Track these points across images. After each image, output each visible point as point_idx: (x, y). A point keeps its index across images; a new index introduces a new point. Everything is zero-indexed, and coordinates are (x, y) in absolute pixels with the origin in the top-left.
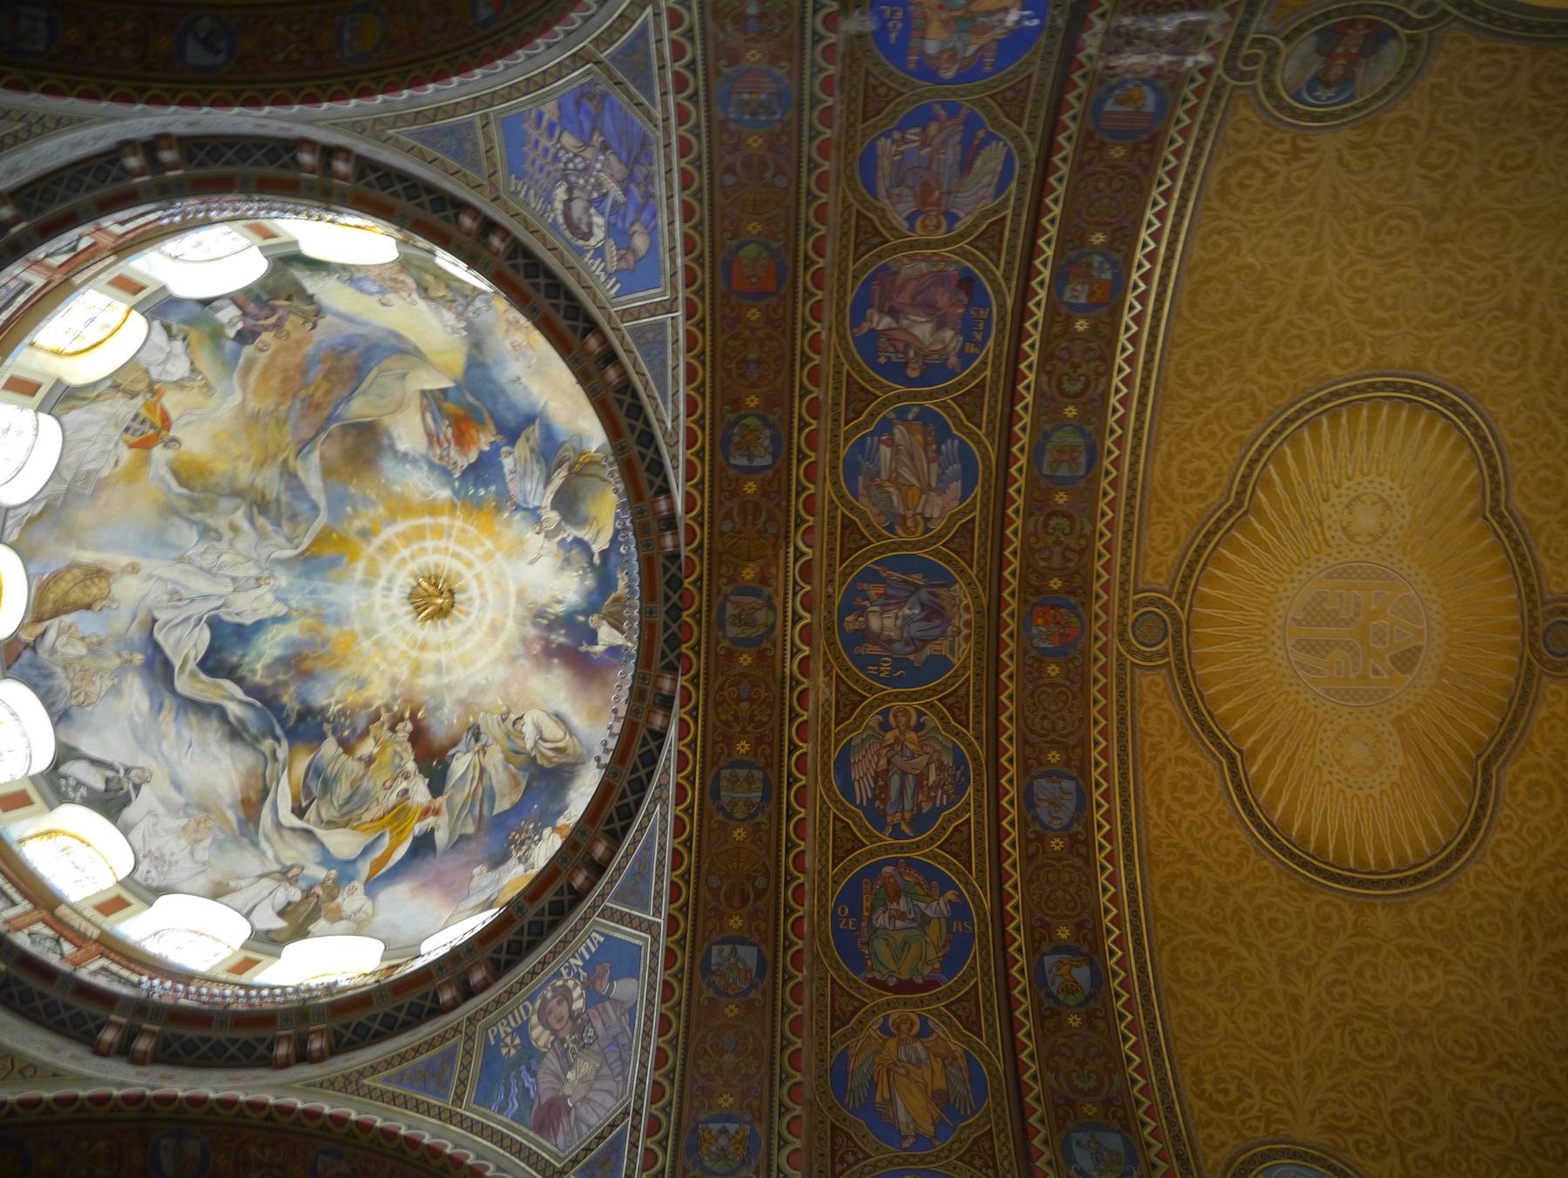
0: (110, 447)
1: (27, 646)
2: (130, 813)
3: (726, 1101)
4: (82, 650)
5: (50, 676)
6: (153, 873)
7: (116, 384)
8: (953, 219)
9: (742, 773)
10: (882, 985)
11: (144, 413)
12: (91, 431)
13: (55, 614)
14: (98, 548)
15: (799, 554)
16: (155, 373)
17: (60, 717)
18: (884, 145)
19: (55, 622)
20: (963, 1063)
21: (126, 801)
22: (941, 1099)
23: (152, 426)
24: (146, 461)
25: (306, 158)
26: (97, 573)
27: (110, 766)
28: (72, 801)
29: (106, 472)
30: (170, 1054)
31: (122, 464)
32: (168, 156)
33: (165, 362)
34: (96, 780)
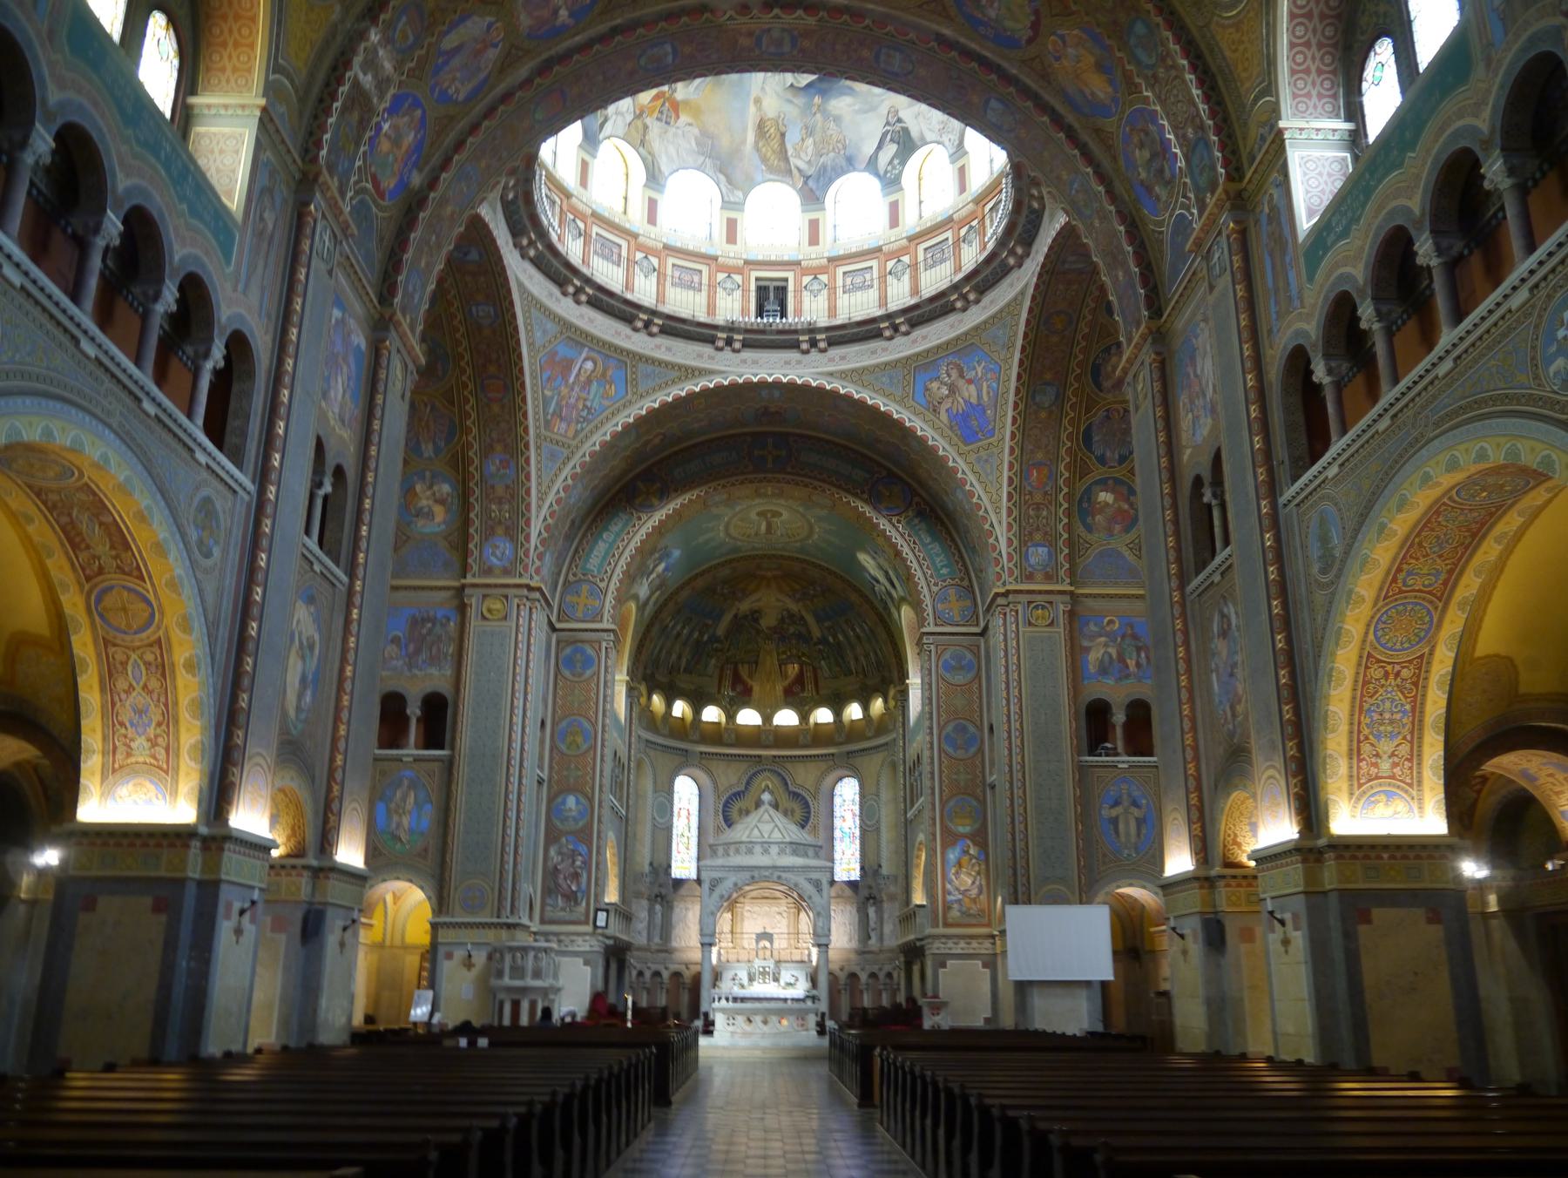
0: (680, 132)
1: (805, 183)
2: (914, 134)
3: (1065, 176)
4: (810, 141)
5: (824, 168)
6: (952, 138)
7: (640, 142)
8: (490, 26)
9: (882, 58)
10: (1030, 41)
11: (655, 115)
12: (672, 150)
13: (787, 160)
14: (745, 130)
15: (731, 18)
16: (629, 118)
17: (850, 164)
18: (461, 97)
19: (791, 160)
20: (1084, 36)
21: (906, 131)
22: (1100, 67)
23: (663, 105)
24: (686, 102)
25: (511, 196)
26: (761, 128)
27: (884, 135)
28: (901, 172)
29: (696, 131)
30: (1028, 241)
31: (690, 120)
32: (525, 242)
33: (622, 114)
34: (891, 149)
